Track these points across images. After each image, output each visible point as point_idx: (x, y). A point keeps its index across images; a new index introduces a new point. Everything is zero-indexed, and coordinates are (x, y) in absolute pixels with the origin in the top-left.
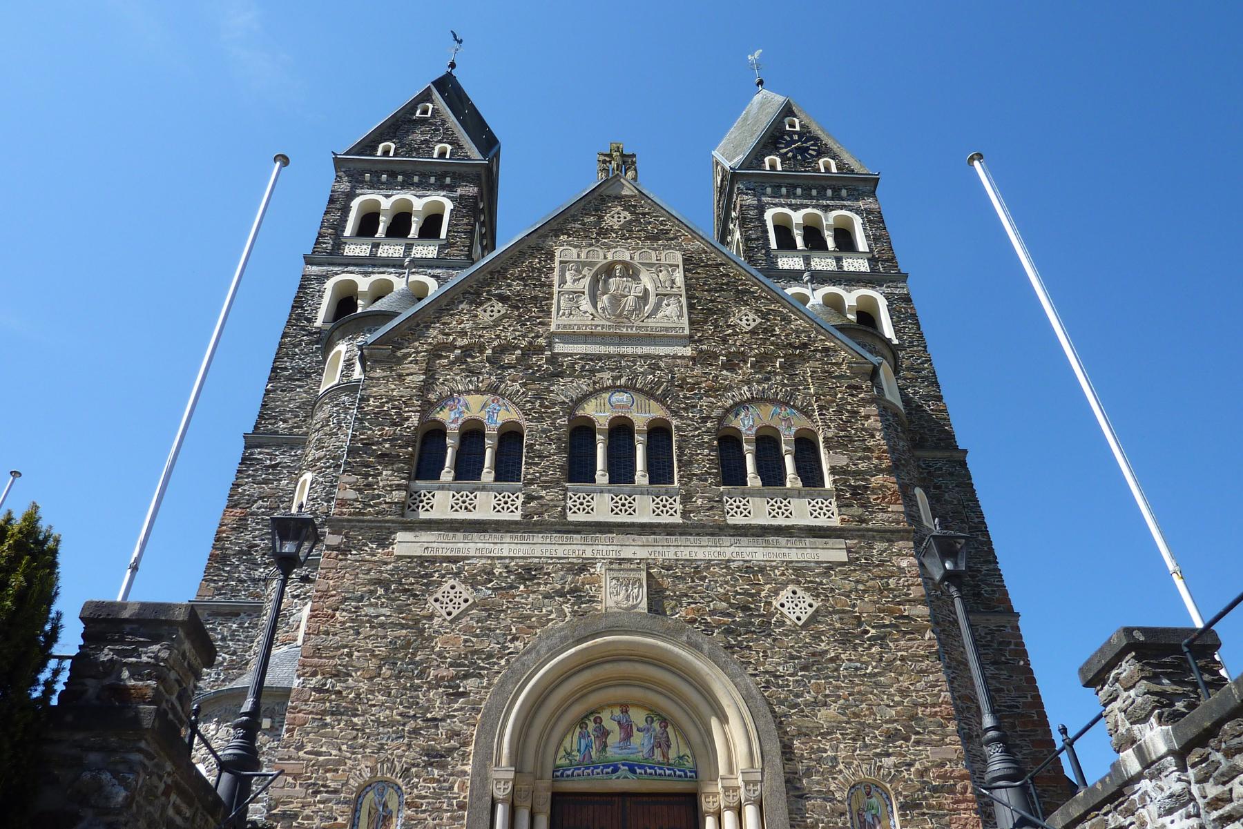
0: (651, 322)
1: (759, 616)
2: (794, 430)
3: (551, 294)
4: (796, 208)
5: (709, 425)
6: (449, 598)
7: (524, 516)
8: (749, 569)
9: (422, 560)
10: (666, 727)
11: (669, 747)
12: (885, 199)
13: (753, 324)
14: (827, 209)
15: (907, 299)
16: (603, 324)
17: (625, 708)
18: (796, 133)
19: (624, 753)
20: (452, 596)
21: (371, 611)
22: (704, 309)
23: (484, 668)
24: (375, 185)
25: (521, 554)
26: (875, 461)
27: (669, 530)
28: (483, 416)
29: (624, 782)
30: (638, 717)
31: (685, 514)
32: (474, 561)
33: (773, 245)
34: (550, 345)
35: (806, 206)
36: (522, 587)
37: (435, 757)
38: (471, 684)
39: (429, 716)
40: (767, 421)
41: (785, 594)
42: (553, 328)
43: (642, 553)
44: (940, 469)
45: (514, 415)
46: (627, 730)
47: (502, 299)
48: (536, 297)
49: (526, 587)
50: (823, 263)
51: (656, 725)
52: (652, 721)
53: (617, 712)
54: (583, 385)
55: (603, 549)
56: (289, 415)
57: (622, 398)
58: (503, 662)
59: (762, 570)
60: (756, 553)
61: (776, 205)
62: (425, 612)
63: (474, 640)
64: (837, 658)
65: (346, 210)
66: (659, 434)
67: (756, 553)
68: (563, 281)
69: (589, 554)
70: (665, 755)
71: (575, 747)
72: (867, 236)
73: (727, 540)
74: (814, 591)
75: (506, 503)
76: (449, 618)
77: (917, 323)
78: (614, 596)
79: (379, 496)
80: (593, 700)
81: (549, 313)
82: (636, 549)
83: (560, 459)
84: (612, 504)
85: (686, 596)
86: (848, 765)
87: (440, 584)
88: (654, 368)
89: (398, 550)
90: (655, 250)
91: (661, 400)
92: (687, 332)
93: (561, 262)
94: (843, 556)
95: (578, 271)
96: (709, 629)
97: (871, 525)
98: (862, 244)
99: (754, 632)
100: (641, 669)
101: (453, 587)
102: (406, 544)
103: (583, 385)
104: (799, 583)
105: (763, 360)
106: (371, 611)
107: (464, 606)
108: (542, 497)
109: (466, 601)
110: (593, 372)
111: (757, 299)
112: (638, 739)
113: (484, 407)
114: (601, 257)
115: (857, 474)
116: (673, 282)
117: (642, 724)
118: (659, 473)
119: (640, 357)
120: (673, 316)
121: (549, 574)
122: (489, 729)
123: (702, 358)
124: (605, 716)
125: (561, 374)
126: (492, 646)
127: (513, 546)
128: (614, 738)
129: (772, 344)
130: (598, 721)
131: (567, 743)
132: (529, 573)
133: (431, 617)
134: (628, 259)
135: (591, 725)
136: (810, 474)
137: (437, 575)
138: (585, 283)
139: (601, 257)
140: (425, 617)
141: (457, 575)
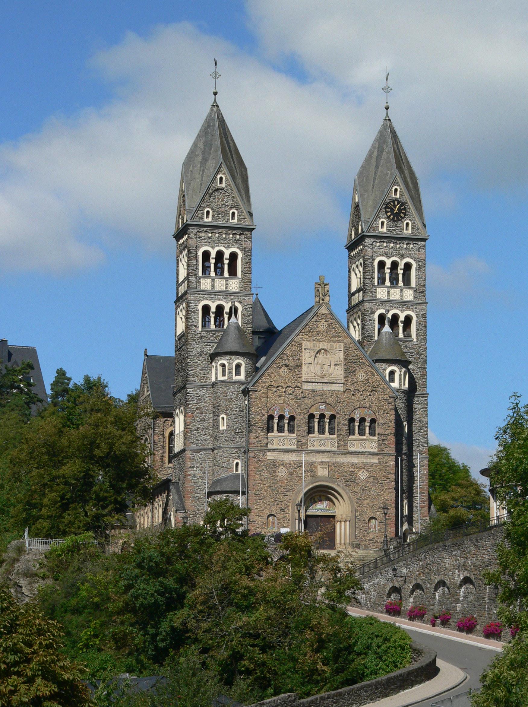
2: (370, 418)
3: (302, 364)
4: (388, 257)
5: (346, 417)
6: (282, 472)
7: (297, 447)
8: (353, 465)
13: (363, 378)
14: (402, 257)
15: (424, 316)
21: (264, 474)
22: (349, 373)
24: (208, 243)
27: (334, 453)
31: (338, 447)
33: (376, 284)
35: (393, 256)
38: (288, 493)
43: (327, 460)
44: (418, 401)
47: (287, 366)
50: (395, 294)
55: (318, 458)
56: (198, 374)
60: (355, 460)
61: (381, 255)
64: (371, 489)
65: (196, 258)
67: (355, 460)
69: (314, 460)
73: (349, 456)
77: (426, 330)
79: (260, 441)
80: (314, 495)
81: (301, 374)
82: (326, 458)
83: (306, 429)
86: (369, 513)
90: (335, 342)
97: (385, 452)
102: (270, 456)
104: (364, 468)
106: (264, 474)
111: (365, 366)
115: (385, 435)
118: (332, 432)
120: (339, 373)
124: (316, 498)
129: (368, 386)
133: (277, 476)
134: (326, 348)
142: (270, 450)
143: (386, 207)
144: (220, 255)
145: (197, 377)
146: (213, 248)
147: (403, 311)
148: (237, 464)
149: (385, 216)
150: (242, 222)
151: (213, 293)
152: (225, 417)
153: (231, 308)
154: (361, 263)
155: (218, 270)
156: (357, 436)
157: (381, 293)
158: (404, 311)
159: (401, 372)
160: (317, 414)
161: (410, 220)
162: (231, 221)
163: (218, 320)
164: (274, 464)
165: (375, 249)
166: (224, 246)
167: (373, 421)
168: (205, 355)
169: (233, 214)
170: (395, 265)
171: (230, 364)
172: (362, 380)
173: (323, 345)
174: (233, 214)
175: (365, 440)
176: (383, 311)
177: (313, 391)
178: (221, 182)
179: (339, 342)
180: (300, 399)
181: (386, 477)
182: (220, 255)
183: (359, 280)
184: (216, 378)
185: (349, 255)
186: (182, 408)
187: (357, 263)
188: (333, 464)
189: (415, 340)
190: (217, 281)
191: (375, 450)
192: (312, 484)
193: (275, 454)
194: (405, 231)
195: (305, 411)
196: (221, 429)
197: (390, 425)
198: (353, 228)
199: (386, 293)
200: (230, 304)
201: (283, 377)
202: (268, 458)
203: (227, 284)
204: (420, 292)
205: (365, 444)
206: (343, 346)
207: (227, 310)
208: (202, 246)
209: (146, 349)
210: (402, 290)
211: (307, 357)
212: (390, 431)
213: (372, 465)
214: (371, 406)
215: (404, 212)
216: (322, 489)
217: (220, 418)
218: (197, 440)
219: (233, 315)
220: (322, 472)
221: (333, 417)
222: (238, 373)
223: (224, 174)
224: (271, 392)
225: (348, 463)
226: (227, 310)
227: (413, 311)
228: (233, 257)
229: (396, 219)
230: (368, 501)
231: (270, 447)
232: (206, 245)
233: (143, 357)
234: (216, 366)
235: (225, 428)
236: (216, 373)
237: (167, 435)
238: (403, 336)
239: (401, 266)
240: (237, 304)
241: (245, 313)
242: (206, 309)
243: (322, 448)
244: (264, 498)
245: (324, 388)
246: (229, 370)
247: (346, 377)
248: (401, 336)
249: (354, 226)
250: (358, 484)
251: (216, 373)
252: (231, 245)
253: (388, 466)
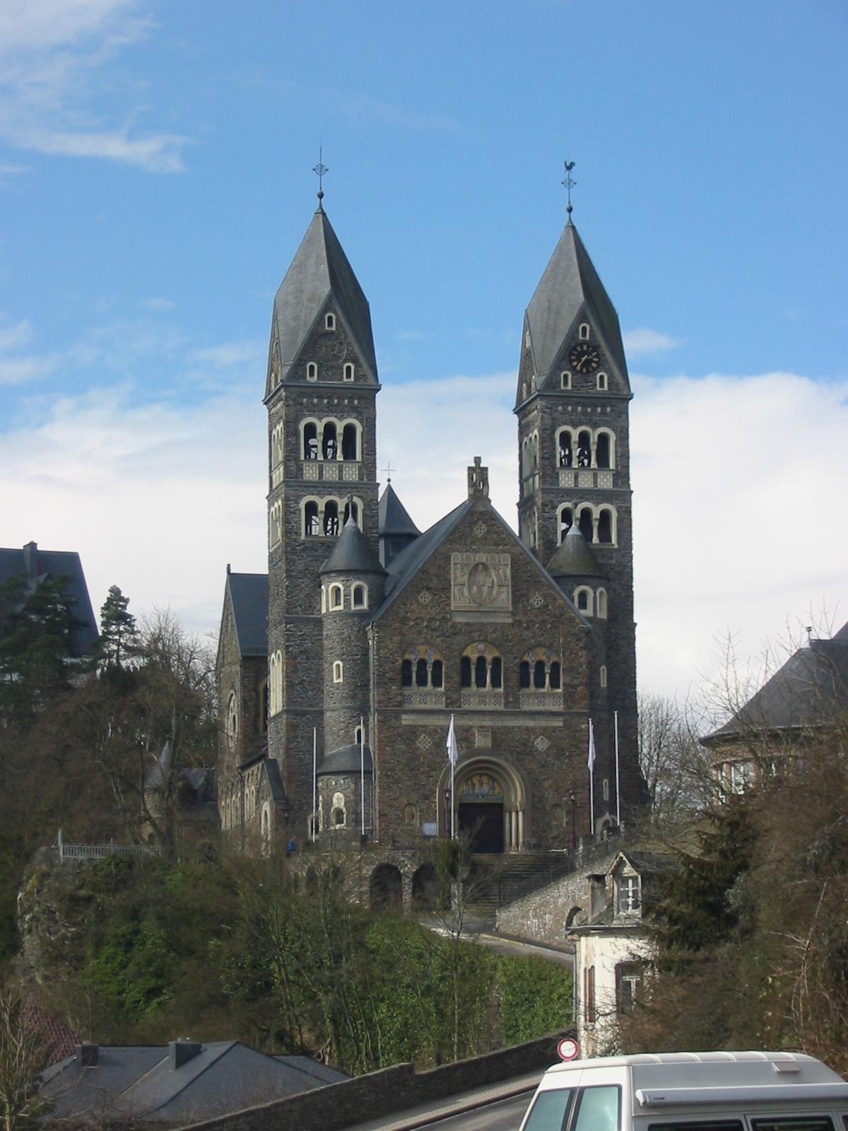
2: (551, 662)
4: (575, 426)
7: (447, 706)
9: (412, 726)
14: (595, 426)
16: (473, 606)
18: (585, 342)
19: (482, 790)
24: (313, 410)
26: (581, 680)
29: (480, 800)
30: (485, 779)
35: (581, 424)
37: (426, 797)
38: (434, 773)
41: (539, 739)
42: (452, 608)
43: (490, 723)
45: (438, 657)
46: (481, 784)
47: (428, 589)
51: (491, 783)
55: (475, 722)
56: (301, 602)
57: (481, 646)
60: (530, 723)
65: (296, 434)
67: (530, 723)
68: (456, 578)
69: (471, 724)
70: (494, 792)
72: (616, 453)
74: (549, 738)
78: (481, 741)
79: (391, 699)
80: (472, 774)
82: (488, 722)
83: (457, 679)
88: (495, 631)
91: (498, 648)
92: (510, 609)
94: (561, 724)
95: (462, 569)
98: (612, 466)
100: (488, 765)
104: (543, 735)
105: (544, 622)
113: (426, 651)
115: (574, 687)
116: (506, 576)
118: (496, 683)
120: (504, 598)
123: (517, 623)
125: (456, 634)
129: (548, 615)
130: (472, 781)
134: (485, 561)
135: (469, 782)
136: (555, 684)
138: (465, 579)
141: (425, 732)
142: (406, 712)
143: (571, 354)
144: (330, 430)
145: (300, 606)
146: (320, 419)
147: (597, 504)
148: (359, 732)
149: (569, 367)
150: (361, 382)
151: (321, 486)
152: (341, 664)
153: (347, 506)
154: (536, 436)
155: (329, 450)
156: (532, 688)
157: (566, 480)
158: (599, 503)
159: (595, 593)
160: (474, 657)
161: (606, 372)
162: (345, 380)
163: (330, 523)
164: (413, 731)
165: (556, 415)
166: (336, 417)
167: (555, 666)
168: (311, 574)
169: (349, 368)
170: (584, 438)
171: (347, 587)
172: (538, 606)
173: (482, 557)
174: (349, 368)
175: (544, 694)
176: (568, 505)
177: (467, 624)
178: (330, 324)
179: (504, 552)
180: (448, 637)
181: (575, 746)
182: (330, 430)
183: (533, 459)
184: (327, 609)
185: (520, 424)
186: (279, 652)
187: (530, 435)
189: (616, 546)
190: (327, 468)
191: (559, 707)
192: (469, 758)
193: (412, 717)
194: (598, 388)
195: (455, 654)
196: (335, 681)
197: (580, 670)
198: (524, 385)
199: (573, 479)
200: (346, 500)
201: (423, 605)
202: (403, 723)
203: (341, 471)
204: (622, 475)
205: (547, 700)
206: (509, 559)
207: (341, 508)
208: (304, 416)
209: (229, 565)
210: (595, 476)
211: (458, 575)
212: (581, 680)
213: (555, 729)
214: (552, 644)
215: (597, 360)
216: (483, 765)
217: (334, 665)
218: (302, 698)
219: (350, 515)
220: (481, 741)
221: (496, 661)
222: (358, 600)
223: (335, 312)
224: (407, 627)
225: (519, 727)
226: (341, 508)
227: (612, 504)
228: (350, 430)
229: (584, 370)
230: (550, 782)
231: (407, 706)
232: (310, 416)
233: (225, 575)
234: (327, 591)
235: (341, 680)
236: (327, 602)
237: (261, 688)
238: (598, 542)
239: (594, 439)
240: (356, 500)
241: (368, 512)
242: (311, 509)
243: (482, 707)
244: (397, 781)
245: (485, 620)
246: (345, 596)
247: (515, 602)
248: (595, 539)
249: (526, 381)
250: (534, 758)
251: (327, 602)
252: (345, 415)
253: (578, 731)
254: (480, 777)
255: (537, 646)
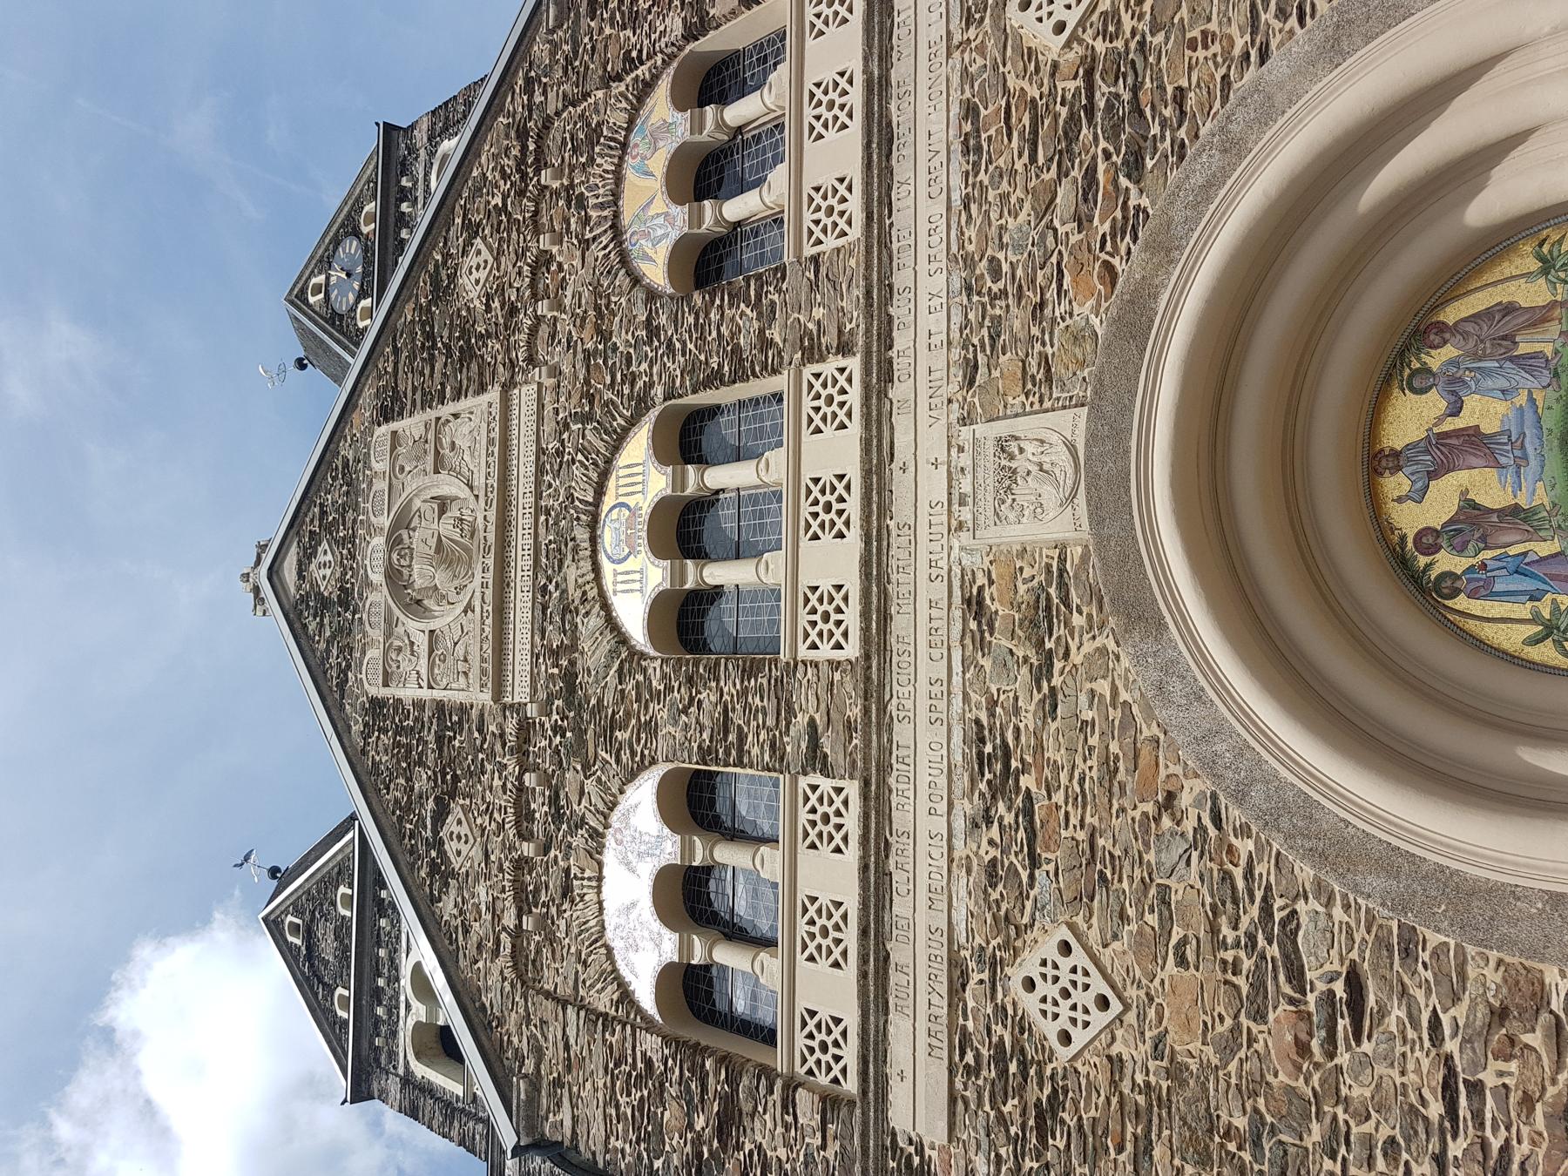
0: (479, 481)
1: (1090, 88)
8: (971, 146)
10: (1442, 328)
11: (1509, 309)
12: (410, 110)
17: (1377, 462)
20: (1053, 991)
23: (1266, 910)
25: (942, 781)
28: (647, 871)
30: (1411, 418)
31: (844, 349)
32: (960, 916)
34: (519, 708)
36: (1026, 781)
39: (1435, 1110)
40: (657, 184)
43: (933, 442)
47: (441, 815)
48: (440, 739)
49: (1025, 768)
52: (1426, 370)
53: (1395, 484)
54: (590, 624)
58: (1245, 846)
59: (970, 111)
62: (1102, 1079)
63: (1177, 934)
66: (688, 440)
71: (1523, 610)
75: (826, 819)
76: (1116, 1006)
84: (827, 538)
85: (1042, 305)
87: (1022, 1026)
89: (933, 1131)
93: (386, 685)
96: (1129, 224)
99: (1135, 90)
101: (1030, 985)
103: (590, 624)
107: (1079, 957)
108: (812, 722)
109: (1065, 948)
110: (566, 609)
112: (1485, 411)
114: (378, 597)
117: (1433, 404)
119: (538, 496)
121: (992, 704)
122: (1476, 902)
124: (1409, 519)
126: (1189, 885)
127: (923, 805)
128: (1489, 488)
130: (1429, 540)
131: (1511, 638)
132: (993, 763)
133: (1116, 1063)
135: (1447, 562)
137: (998, 1029)
139: (378, 597)
140: (1114, 1084)
188: (971, 368)
254: (1396, 459)
255: (616, 230)
